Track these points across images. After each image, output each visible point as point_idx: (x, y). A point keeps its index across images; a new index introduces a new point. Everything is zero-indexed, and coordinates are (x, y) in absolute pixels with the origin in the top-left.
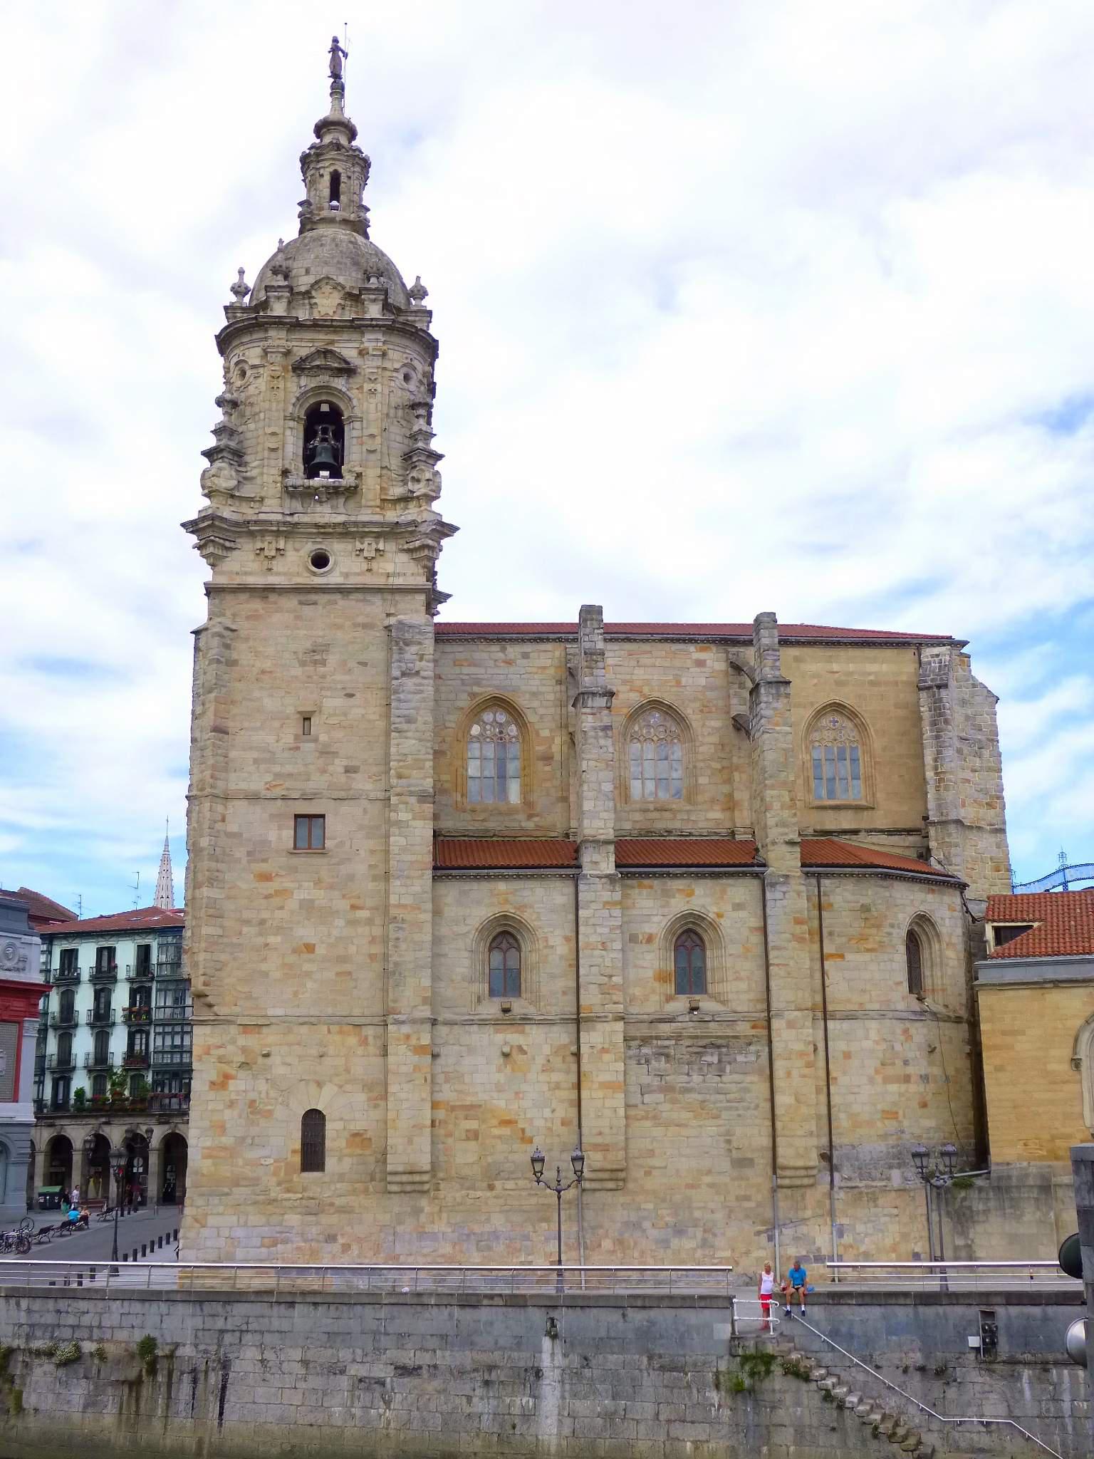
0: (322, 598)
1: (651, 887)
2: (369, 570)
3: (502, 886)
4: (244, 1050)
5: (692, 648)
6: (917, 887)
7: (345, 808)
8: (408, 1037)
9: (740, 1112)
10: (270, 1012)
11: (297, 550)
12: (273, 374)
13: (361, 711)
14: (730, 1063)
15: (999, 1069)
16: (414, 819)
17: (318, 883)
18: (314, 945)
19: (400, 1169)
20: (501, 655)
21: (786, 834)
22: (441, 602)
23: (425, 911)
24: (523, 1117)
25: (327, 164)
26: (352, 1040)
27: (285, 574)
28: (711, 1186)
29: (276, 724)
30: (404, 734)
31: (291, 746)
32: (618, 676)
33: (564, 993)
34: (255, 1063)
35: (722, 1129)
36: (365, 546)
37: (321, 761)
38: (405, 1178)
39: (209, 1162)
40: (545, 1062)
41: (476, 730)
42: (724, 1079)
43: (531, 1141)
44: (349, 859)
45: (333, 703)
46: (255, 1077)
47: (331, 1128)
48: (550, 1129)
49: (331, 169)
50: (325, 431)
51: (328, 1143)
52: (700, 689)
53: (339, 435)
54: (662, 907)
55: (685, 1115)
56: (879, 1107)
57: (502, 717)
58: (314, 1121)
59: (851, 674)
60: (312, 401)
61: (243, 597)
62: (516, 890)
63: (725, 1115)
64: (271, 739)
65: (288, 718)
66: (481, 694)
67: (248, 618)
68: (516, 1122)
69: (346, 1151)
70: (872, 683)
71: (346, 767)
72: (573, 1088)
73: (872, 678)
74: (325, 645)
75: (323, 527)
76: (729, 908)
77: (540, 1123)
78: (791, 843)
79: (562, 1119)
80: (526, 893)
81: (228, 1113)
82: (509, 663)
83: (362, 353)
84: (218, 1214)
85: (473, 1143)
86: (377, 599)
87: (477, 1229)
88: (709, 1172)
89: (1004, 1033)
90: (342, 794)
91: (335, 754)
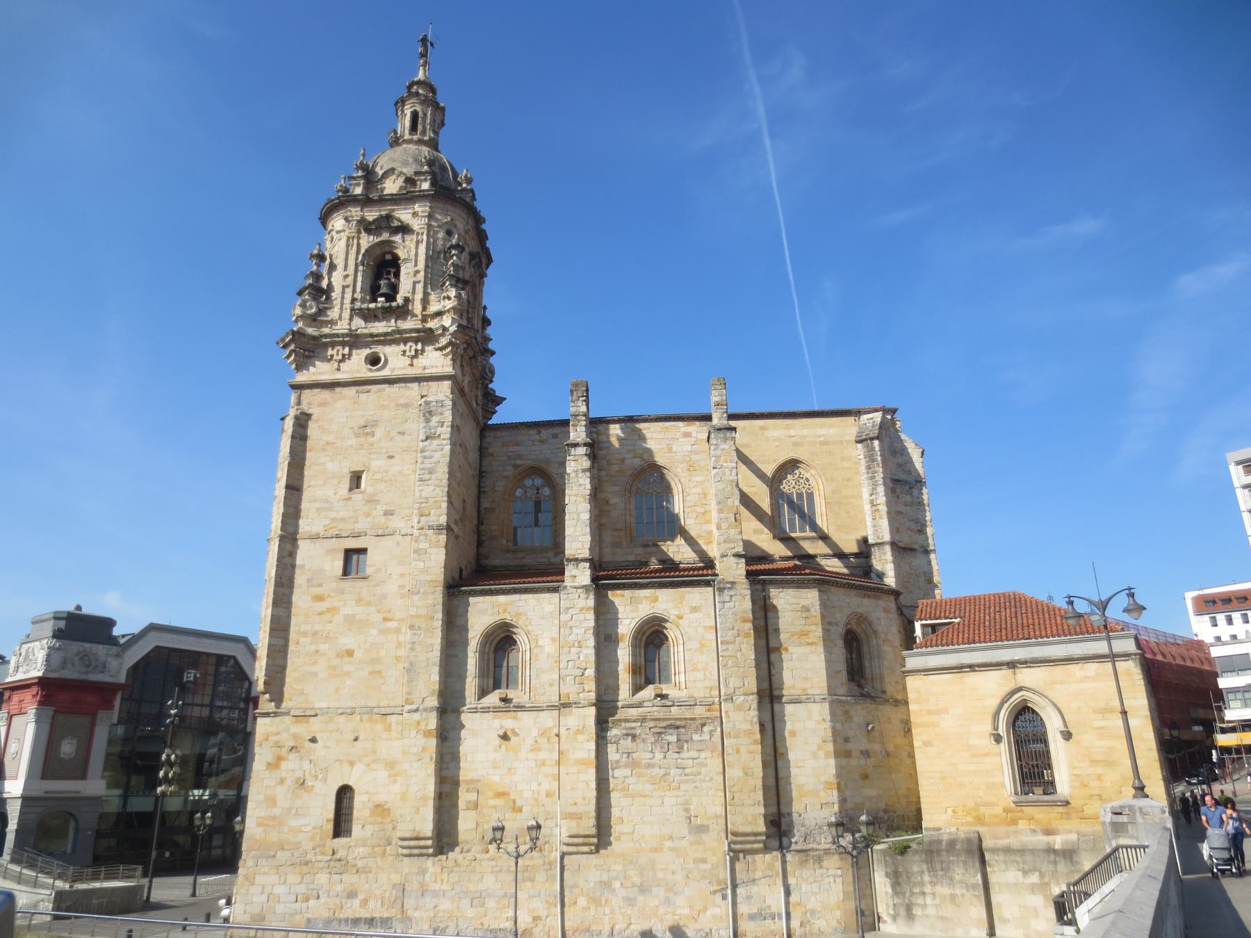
0: (374, 388)
2: (412, 365)
4: (295, 737)
5: (680, 424)
6: (853, 592)
7: (388, 542)
8: (418, 723)
9: (696, 784)
10: (316, 706)
11: (358, 355)
14: (687, 741)
15: (927, 744)
17: (359, 601)
19: (408, 835)
20: (537, 437)
21: (733, 548)
22: (498, 405)
23: (437, 620)
24: (514, 789)
26: (379, 727)
27: (348, 372)
28: (672, 849)
29: (335, 481)
30: (426, 483)
31: (345, 497)
32: (625, 447)
33: (551, 685)
34: (303, 747)
35: (681, 800)
36: (407, 347)
37: (366, 509)
38: (412, 843)
39: (261, 829)
40: (533, 743)
41: (519, 492)
42: (682, 755)
43: (520, 810)
44: (384, 582)
46: (301, 759)
48: (536, 800)
49: (412, 109)
50: (388, 273)
51: (356, 813)
52: (687, 453)
53: (397, 275)
54: (632, 611)
55: (648, 788)
56: (823, 779)
57: (538, 481)
58: (344, 794)
59: (804, 437)
60: (378, 252)
61: (316, 391)
62: (515, 602)
63: (683, 787)
66: (522, 465)
67: (320, 405)
68: (509, 794)
69: (370, 820)
70: (823, 443)
71: (386, 511)
73: (822, 439)
75: (377, 336)
76: (687, 610)
77: (527, 794)
78: (737, 555)
79: (547, 791)
80: (520, 604)
82: (542, 442)
83: (415, 214)
84: (264, 873)
87: (472, 887)
88: (671, 838)
89: (930, 713)
90: (380, 532)
91: (377, 502)
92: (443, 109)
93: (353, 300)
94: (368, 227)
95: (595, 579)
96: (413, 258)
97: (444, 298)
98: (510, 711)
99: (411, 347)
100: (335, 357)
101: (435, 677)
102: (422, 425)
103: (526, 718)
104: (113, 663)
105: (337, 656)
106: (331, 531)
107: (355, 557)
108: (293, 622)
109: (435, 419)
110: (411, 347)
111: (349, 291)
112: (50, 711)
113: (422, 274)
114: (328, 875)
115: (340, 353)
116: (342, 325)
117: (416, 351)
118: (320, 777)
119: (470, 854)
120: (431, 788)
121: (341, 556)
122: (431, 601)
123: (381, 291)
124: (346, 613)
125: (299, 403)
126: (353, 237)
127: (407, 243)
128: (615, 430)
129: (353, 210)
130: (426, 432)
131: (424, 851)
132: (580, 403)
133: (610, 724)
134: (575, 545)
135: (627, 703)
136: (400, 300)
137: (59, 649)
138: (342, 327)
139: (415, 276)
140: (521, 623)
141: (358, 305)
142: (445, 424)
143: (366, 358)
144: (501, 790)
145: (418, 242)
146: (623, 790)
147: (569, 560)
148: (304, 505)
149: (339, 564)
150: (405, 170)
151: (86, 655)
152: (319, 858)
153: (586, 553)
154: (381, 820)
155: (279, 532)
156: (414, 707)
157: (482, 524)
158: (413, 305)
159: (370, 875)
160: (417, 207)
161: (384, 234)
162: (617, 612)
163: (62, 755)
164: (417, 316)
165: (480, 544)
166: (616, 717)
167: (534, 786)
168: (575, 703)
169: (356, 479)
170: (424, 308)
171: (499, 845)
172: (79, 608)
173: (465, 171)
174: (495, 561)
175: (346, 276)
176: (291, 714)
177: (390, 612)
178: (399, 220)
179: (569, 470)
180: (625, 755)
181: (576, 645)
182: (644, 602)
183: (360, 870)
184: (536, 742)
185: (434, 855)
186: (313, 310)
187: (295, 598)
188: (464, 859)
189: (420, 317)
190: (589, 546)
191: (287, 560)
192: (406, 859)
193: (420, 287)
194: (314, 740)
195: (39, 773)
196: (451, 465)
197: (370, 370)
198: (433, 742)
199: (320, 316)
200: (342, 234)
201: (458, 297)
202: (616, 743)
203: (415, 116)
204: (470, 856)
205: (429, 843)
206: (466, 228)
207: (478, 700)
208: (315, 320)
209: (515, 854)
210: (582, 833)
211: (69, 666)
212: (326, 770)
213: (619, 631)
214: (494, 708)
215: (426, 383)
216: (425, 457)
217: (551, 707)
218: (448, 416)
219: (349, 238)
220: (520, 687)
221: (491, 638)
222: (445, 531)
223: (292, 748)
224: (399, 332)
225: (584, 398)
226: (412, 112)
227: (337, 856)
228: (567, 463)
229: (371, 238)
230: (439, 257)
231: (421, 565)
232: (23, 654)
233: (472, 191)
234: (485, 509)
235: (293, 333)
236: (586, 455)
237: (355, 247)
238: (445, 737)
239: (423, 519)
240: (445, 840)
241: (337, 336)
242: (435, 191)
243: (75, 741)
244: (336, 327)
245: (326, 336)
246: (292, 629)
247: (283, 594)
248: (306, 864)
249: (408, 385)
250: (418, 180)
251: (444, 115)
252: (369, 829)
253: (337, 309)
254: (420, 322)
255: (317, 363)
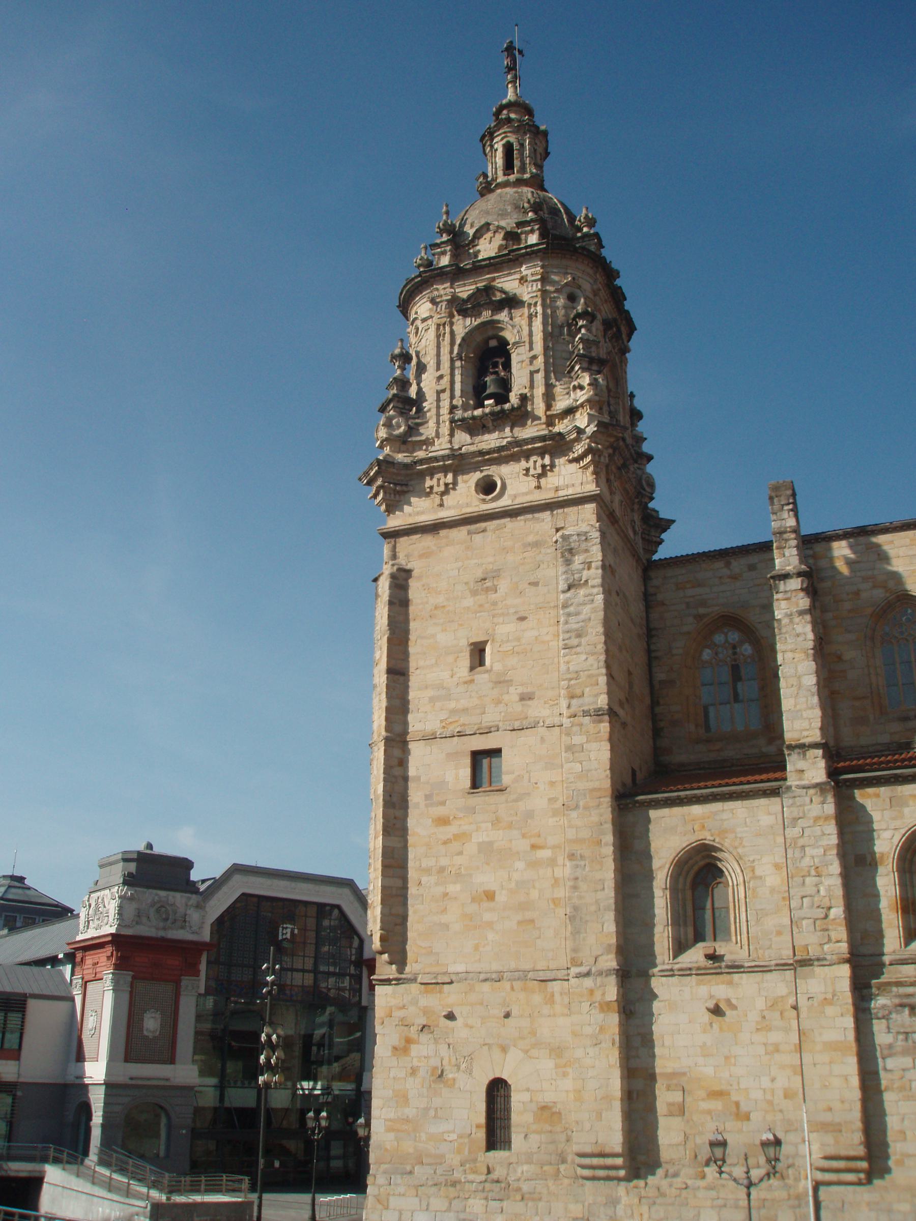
0: (491, 525)
1: (877, 796)
2: (539, 487)
3: (697, 810)
4: (426, 1011)
7: (528, 739)
8: (591, 992)
10: (451, 969)
11: (466, 482)
12: (439, 321)
13: (535, 633)
16: (587, 742)
17: (496, 822)
18: (494, 892)
19: (588, 1149)
20: (726, 571)
22: (664, 530)
23: (606, 844)
25: (499, 138)
26: (537, 998)
29: (450, 659)
30: (574, 650)
33: (779, 933)
34: (437, 1026)
36: (531, 464)
38: (595, 1161)
39: (391, 1136)
41: (707, 654)
43: (747, 1117)
44: (529, 794)
45: (506, 628)
46: (436, 1041)
47: (518, 1100)
48: (770, 1103)
49: (504, 142)
50: (495, 365)
51: (515, 1118)
53: (507, 366)
54: (894, 819)
57: (734, 636)
60: (479, 338)
61: (415, 537)
64: (446, 675)
65: (462, 652)
67: (421, 556)
68: (729, 1094)
69: (534, 1127)
72: (796, 1051)
74: (496, 571)
75: (489, 452)
77: (757, 1095)
80: (724, 816)
81: (410, 1080)
82: (734, 578)
83: (523, 280)
84: (400, 1195)
85: (678, 1120)
86: (546, 515)
90: (517, 725)
91: (509, 682)
92: (545, 134)
93: (453, 408)
94: (460, 307)
95: (833, 773)
96: (527, 339)
97: (575, 388)
98: (721, 973)
99: (535, 462)
100: (436, 489)
101: (610, 927)
102: (561, 569)
103: (746, 984)
104: (194, 916)
105: (474, 900)
106: (451, 728)
107: (485, 762)
108: (411, 856)
109: (578, 559)
110: (535, 462)
111: (446, 396)
112: (128, 976)
113: (540, 360)
114: (483, 1202)
115: (442, 482)
116: (440, 445)
117: (544, 466)
118: (463, 1066)
119: (679, 1180)
120: (615, 1084)
121: (468, 761)
122: (595, 818)
123: (488, 392)
124: (481, 840)
125: (394, 556)
126: (444, 324)
127: (517, 320)
128: (841, 550)
129: (440, 287)
130: (567, 579)
131: (612, 1173)
132: (785, 515)
133: (874, 990)
134: (798, 725)
135: (898, 957)
136: (514, 399)
137: (131, 899)
138: (441, 447)
139: (531, 363)
140: (727, 843)
141: (459, 414)
142: (593, 565)
143: (477, 485)
144: (717, 1088)
145: (530, 317)
146: (902, 1089)
147: (791, 747)
148: (412, 695)
149: (466, 772)
150: (503, 223)
151: (162, 906)
152: (471, 1177)
153: (814, 735)
154: (549, 1128)
155: (384, 733)
156: (583, 969)
157: (658, 704)
158: (533, 404)
159: (541, 1204)
160: (525, 270)
161: (484, 313)
162: (870, 821)
163: (145, 1033)
164: (539, 418)
165: (657, 733)
166: (884, 979)
167: (765, 1082)
168: (818, 960)
169: (478, 653)
170: (549, 407)
171: (720, 1167)
172: (150, 846)
173: (584, 211)
174: (680, 757)
175: (440, 377)
176: (419, 980)
177: (539, 836)
178: (502, 291)
179: (778, 614)
180: (901, 1037)
181: (813, 872)
182: (911, 803)
183: (527, 1196)
184: (764, 1017)
185: (628, 1179)
186: (402, 429)
187: (411, 822)
188: (671, 1186)
189: (544, 419)
190: (819, 724)
191: (397, 771)
192: (588, 1183)
193: (539, 378)
194: (450, 1016)
195: (122, 1056)
196: (606, 622)
197: (484, 500)
198: (614, 1020)
199: (411, 436)
200: (429, 322)
201: (594, 384)
202: (886, 1017)
203: (508, 150)
204: (678, 1182)
205: (619, 1161)
206: (595, 287)
207: (674, 958)
208: (405, 442)
209: (745, 1182)
210: (843, 1153)
211: (144, 920)
212: (470, 1057)
213: (877, 849)
214: (698, 968)
215: (560, 511)
216: (569, 615)
217: (782, 966)
218: (596, 553)
219: (438, 325)
220: (734, 938)
221: (686, 868)
222: (606, 718)
223: (424, 1027)
224: (517, 443)
225: (791, 507)
226: (504, 146)
227: (494, 1176)
228: (775, 604)
229: (468, 321)
230: (561, 334)
231: (577, 767)
232: (93, 905)
233: (597, 235)
234: (660, 682)
235: (379, 463)
236: (802, 589)
237: (447, 336)
238: (631, 1011)
239: (574, 702)
240: (642, 1158)
241: (436, 459)
242: (547, 244)
243: (158, 1015)
244: (433, 449)
245: (421, 461)
246: (411, 864)
247: (395, 818)
248: (454, 1184)
249: (536, 515)
250: (522, 233)
251: (547, 141)
252: (534, 1139)
253: (432, 424)
254: (544, 426)
255: (413, 500)
